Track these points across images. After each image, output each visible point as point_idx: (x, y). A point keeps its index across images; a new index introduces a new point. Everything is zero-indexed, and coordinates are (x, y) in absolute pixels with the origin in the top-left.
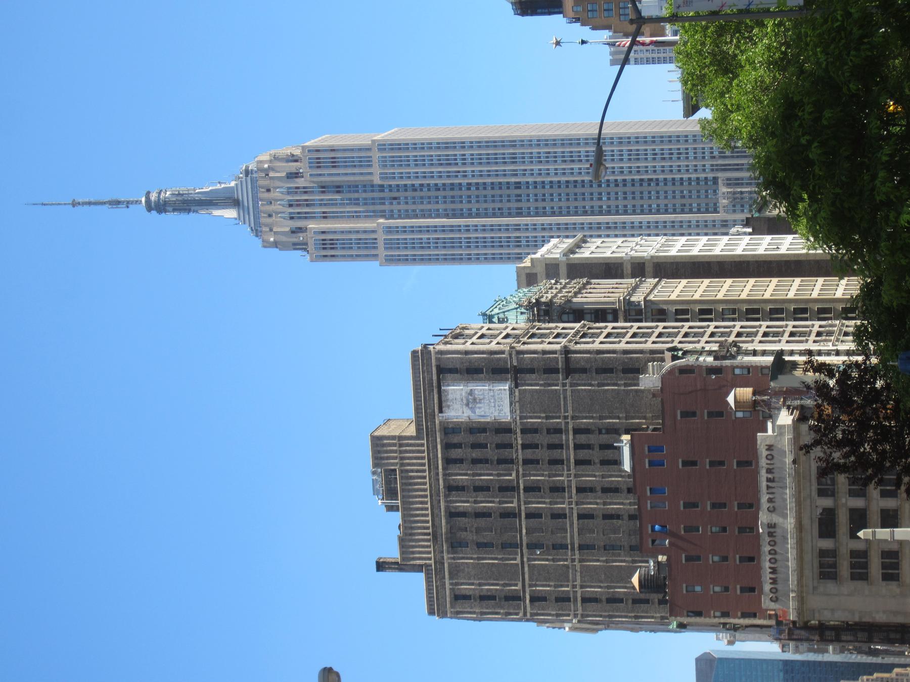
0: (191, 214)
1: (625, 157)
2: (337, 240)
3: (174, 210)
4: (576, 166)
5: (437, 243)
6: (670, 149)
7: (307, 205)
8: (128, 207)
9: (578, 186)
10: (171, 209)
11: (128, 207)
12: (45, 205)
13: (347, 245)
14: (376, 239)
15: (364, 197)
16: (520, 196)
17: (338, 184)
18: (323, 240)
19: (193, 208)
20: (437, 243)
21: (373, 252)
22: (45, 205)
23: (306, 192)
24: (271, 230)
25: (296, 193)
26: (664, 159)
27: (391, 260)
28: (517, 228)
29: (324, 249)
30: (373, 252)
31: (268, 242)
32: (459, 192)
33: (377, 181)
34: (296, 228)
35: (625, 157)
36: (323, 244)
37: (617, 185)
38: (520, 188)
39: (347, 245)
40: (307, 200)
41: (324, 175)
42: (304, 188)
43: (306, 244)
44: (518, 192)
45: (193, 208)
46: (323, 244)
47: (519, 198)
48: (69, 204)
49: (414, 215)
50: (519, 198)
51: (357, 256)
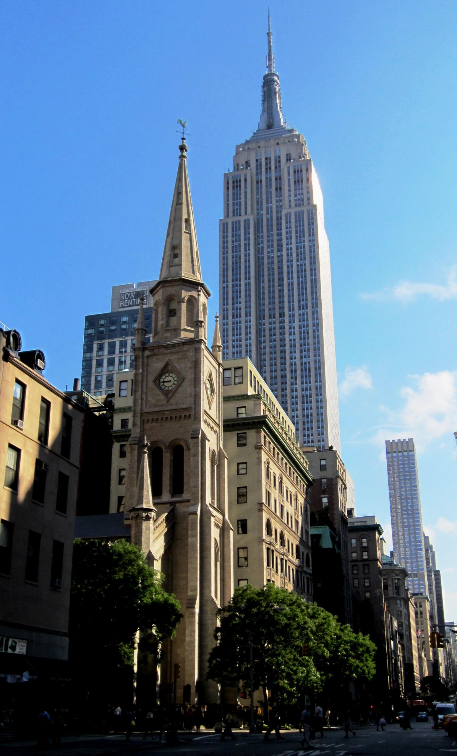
0: (261, 102)
1: (305, 393)
2: (240, 190)
4: (298, 355)
5: (236, 257)
6: (312, 428)
8: (267, 67)
9: (282, 360)
10: (265, 89)
11: (267, 67)
12: (269, 18)
13: (236, 196)
15: (273, 207)
16: (274, 317)
20: (236, 257)
21: (231, 214)
22: (269, 18)
26: (304, 423)
27: (224, 226)
28: (248, 314)
29: (233, 182)
30: (231, 214)
32: (275, 258)
33: (284, 212)
35: (305, 393)
37: (283, 390)
39: (236, 196)
40: (270, 168)
43: (238, 170)
44: (277, 315)
45: (266, 103)
47: (272, 317)
48: (269, 29)
49: (260, 242)
50: (272, 317)
51: (228, 205)
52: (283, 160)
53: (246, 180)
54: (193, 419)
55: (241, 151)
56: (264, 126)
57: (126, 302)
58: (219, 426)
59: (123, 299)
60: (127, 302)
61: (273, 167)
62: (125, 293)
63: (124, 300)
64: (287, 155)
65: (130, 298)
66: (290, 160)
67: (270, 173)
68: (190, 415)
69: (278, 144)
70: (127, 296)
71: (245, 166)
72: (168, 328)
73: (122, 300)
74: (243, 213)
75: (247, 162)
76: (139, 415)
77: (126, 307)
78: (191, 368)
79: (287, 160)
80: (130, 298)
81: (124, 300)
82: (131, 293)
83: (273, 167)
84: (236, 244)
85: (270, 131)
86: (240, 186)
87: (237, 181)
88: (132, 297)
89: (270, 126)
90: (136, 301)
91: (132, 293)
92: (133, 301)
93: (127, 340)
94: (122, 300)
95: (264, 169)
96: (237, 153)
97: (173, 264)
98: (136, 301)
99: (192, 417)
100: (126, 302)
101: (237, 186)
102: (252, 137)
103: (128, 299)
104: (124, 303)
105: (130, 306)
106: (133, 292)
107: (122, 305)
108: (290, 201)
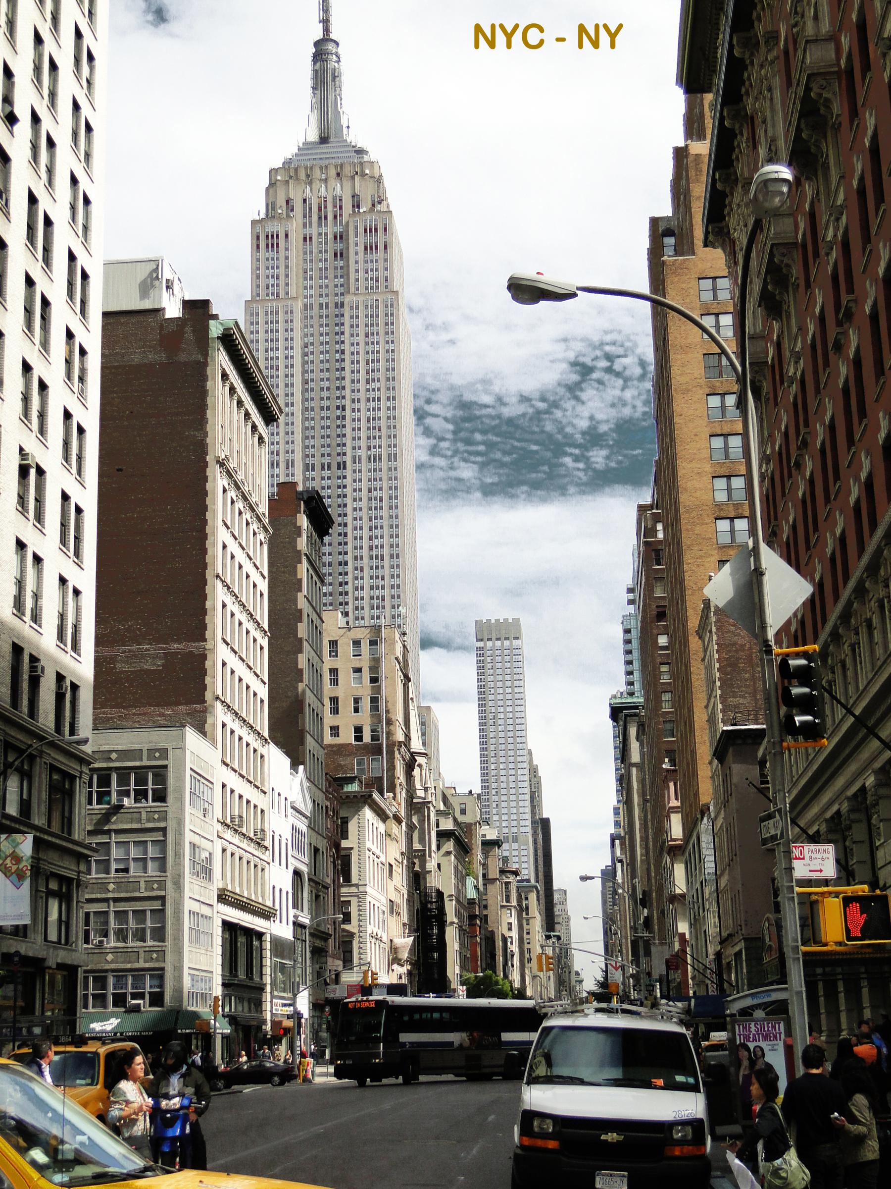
0: (310, 91)
3: (316, 72)
7: (320, 218)
17: (344, 255)
18: (278, 236)
19: (318, 92)
23: (335, 217)
24: (291, 177)
25: (335, 206)
29: (267, 237)
30: (262, 292)
31: (276, 174)
34: (293, 206)
36: (272, 236)
38: (339, 468)
40: (326, 218)
41: (356, 236)
42: (341, 215)
45: (318, 92)
46: (272, 236)
56: (313, 136)
61: (330, 217)
64: (353, 196)
66: (358, 207)
67: (326, 225)
71: (284, 208)
75: (288, 202)
83: (330, 217)
85: (324, 148)
89: (324, 140)
95: (315, 217)
96: (272, 185)
101: (272, 245)
102: (296, 155)
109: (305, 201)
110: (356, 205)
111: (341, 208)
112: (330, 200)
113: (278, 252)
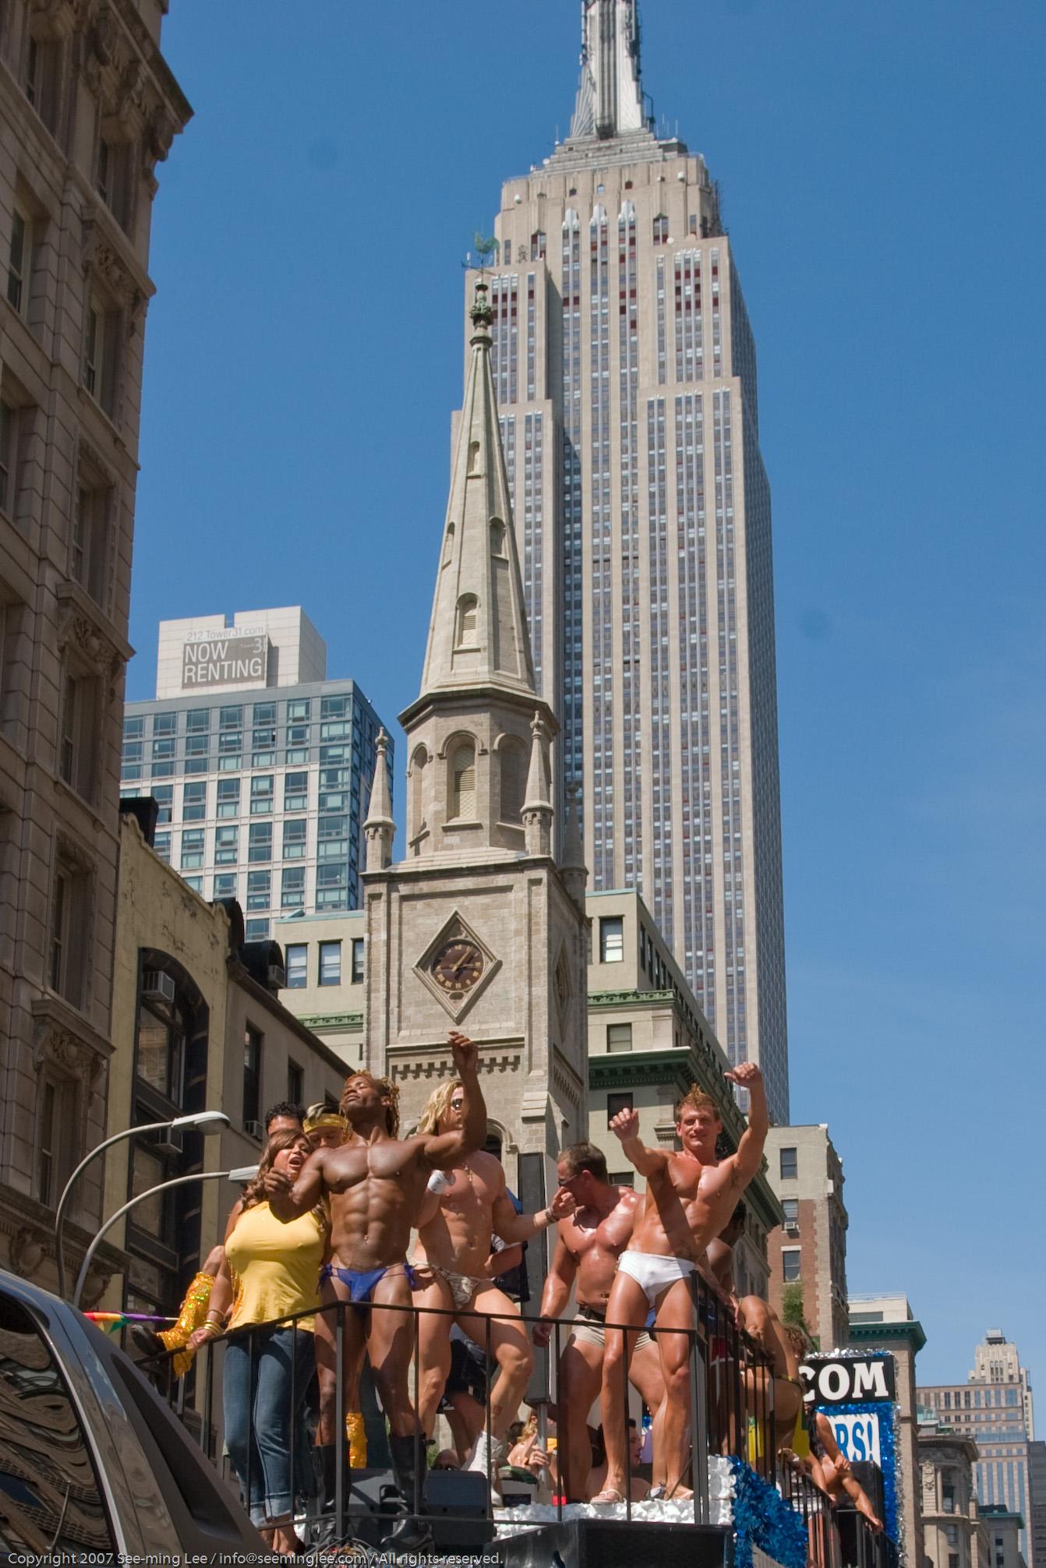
14: (514, 402)
18: (514, 296)
23: (622, 259)
25: (622, 240)
46: (505, 297)
52: (644, 235)
53: (531, 294)
54: (527, 1069)
55: (519, 202)
57: (202, 669)
58: (582, 1084)
59: (194, 660)
60: (207, 669)
62: (199, 644)
63: (196, 664)
65: (215, 657)
66: (665, 238)
68: (517, 1058)
69: (629, 185)
70: (204, 651)
72: (454, 822)
73: (191, 662)
74: (522, 396)
75: (534, 238)
76: (382, 1055)
77: (201, 685)
78: (518, 933)
79: (656, 238)
80: (215, 657)
81: (196, 664)
82: (216, 643)
84: (694, 638)
86: (514, 312)
87: (505, 297)
88: (219, 656)
90: (230, 666)
91: (220, 645)
92: (222, 667)
93: (205, 783)
94: (191, 662)
97: (463, 647)
98: (230, 666)
99: (524, 1062)
100: (202, 669)
103: (208, 662)
104: (196, 674)
105: (213, 682)
106: (223, 642)
107: (190, 678)
108: (662, 365)
109: (565, 234)
110: (661, 238)
111: (633, 241)
112: (614, 230)
113: (514, 324)
